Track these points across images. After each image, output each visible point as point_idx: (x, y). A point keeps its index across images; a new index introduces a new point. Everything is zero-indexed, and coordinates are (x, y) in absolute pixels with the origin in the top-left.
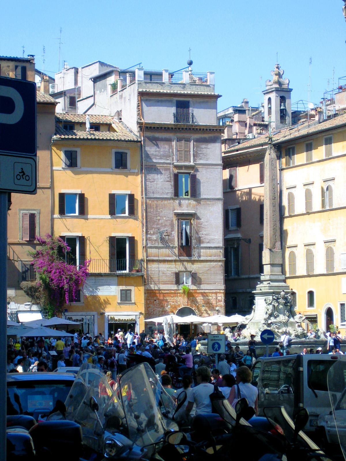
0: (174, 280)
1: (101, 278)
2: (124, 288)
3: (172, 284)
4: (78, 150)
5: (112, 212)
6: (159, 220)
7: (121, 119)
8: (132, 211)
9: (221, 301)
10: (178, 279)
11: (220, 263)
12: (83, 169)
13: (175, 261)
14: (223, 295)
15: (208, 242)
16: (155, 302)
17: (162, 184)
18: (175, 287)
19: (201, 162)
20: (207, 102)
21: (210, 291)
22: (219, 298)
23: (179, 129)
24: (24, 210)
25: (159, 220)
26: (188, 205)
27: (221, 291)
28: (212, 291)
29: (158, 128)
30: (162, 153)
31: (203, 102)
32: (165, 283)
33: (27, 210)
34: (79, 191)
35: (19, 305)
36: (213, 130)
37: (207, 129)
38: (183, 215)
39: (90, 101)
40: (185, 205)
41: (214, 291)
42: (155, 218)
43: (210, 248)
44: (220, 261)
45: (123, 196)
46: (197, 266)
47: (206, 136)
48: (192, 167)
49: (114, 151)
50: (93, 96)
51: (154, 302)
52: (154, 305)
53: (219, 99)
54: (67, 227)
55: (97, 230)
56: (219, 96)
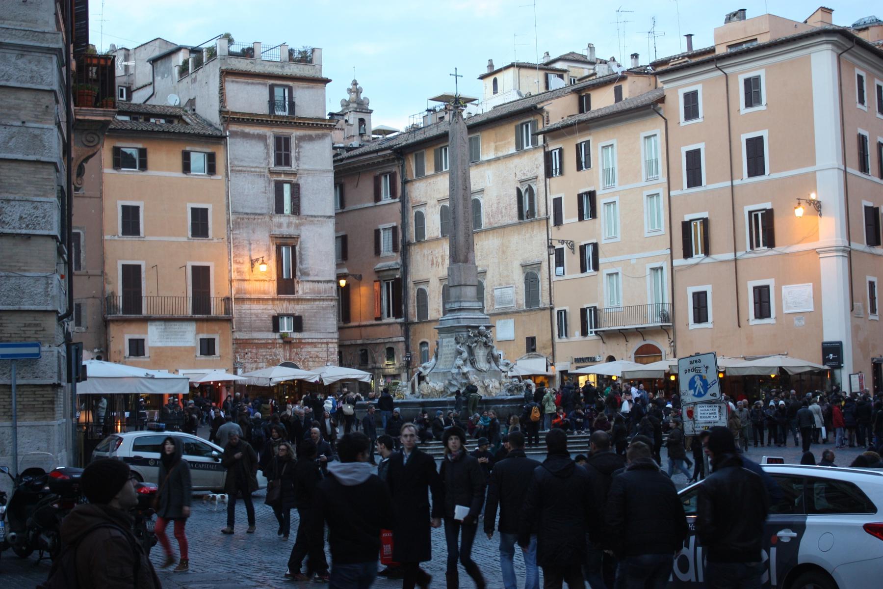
0: (271, 325)
3: (269, 331)
7: (194, 110)
13: (273, 299)
14: (336, 346)
15: (317, 275)
19: (306, 167)
20: (312, 88)
22: (331, 350)
26: (289, 225)
27: (334, 341)
31: (308, 88)
32: (260, 330)
39: (148, 91)
40: (285, 225)
41: (325, 341)
43: (318, 282)
47: (313, 133)
48: (294, 174)
50: (152, 83)
53: (328, 85)
56: (327, 81)
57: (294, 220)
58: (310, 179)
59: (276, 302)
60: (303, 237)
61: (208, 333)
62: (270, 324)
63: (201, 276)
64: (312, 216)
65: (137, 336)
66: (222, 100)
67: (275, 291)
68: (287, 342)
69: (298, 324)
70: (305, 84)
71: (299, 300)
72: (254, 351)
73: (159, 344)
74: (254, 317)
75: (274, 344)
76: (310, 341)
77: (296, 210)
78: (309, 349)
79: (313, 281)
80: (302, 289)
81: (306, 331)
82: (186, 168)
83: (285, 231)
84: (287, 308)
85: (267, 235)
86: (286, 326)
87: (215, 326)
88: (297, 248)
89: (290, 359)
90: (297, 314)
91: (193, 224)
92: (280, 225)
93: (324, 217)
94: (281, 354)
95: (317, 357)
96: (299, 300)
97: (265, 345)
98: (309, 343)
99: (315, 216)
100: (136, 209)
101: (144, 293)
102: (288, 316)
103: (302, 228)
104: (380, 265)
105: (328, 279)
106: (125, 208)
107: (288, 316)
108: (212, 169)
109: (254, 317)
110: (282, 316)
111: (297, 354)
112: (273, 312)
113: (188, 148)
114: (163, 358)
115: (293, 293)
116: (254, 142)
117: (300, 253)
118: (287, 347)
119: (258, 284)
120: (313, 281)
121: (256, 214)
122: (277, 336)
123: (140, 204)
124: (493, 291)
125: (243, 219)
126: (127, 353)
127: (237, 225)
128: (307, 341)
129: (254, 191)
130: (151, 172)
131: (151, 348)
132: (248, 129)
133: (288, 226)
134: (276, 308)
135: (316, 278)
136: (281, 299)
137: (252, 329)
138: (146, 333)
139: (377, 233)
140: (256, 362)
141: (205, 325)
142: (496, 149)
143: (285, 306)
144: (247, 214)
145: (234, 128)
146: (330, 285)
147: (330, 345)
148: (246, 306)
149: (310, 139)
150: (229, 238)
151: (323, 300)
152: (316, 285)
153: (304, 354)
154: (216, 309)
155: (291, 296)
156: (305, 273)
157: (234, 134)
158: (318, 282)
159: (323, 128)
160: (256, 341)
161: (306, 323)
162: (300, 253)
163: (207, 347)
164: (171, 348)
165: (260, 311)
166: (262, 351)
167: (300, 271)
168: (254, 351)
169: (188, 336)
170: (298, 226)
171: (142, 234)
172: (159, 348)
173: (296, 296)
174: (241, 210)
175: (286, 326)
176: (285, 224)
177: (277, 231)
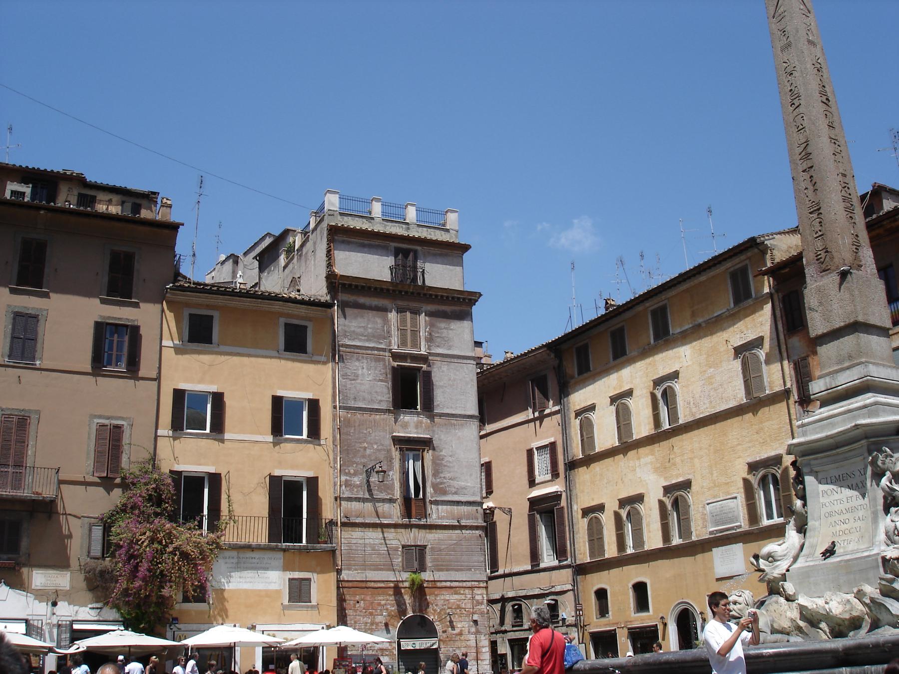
1: (250, 554)
2: (297, 575)
4: (216, 314)
5: (277, 429)
6: (365, 448)
8: (315, 432)
9: (482, 603)
11: (478, 532)
12: (222, 348)
13: (396, 526)
15: (456, 493)
16: (357, 605)
17: (372, 383)
20: (446, 255)
21: (461, 584)
22: (478, 597)
23: (400, 292)
24: (100, 417)
25: (365, 448)
26: (418, 425)
28: (464, 584)
29: (363, 287)
30: (370, 330)
31: (441, 255)
33: (108, 418)
34: (214, 388)
35: (76, 608)
36: (459, 298)
37: (447, 297)
40: (412, 425)
41: (469, 584)
42: (357, 445)
43: (458, 503)
44: (477, 528)
45: (297, 404)
46: (437, 536)
47: (447, 308)
48: (424, 359)
49: (282, 321)
51: (355, 605)
52: (355, 611)
53: (466, 256)
54: (189, 455)
55: (245, 463)
66: (330, 265)
70: (437, 251)
72: (368, 598)
76: (448, 584)
80: (437, 514)
84: (415, 538)
92: (405, 426)
95: (459, 607)
104: (536, 492)
124: (704, 507)
128: (444, 584)
134: (400, 537)
135: (456, 498)
137: (364, 567)
139: (530, 453)
140: (371, 614)
142: (694, 315)
147: (476, 591)
148: (357, 534)
153: (440, 603)
163: (299, 592)
164: (246, 591)
167: (434, 486)
173: (429, 521)
174: (352, 404)
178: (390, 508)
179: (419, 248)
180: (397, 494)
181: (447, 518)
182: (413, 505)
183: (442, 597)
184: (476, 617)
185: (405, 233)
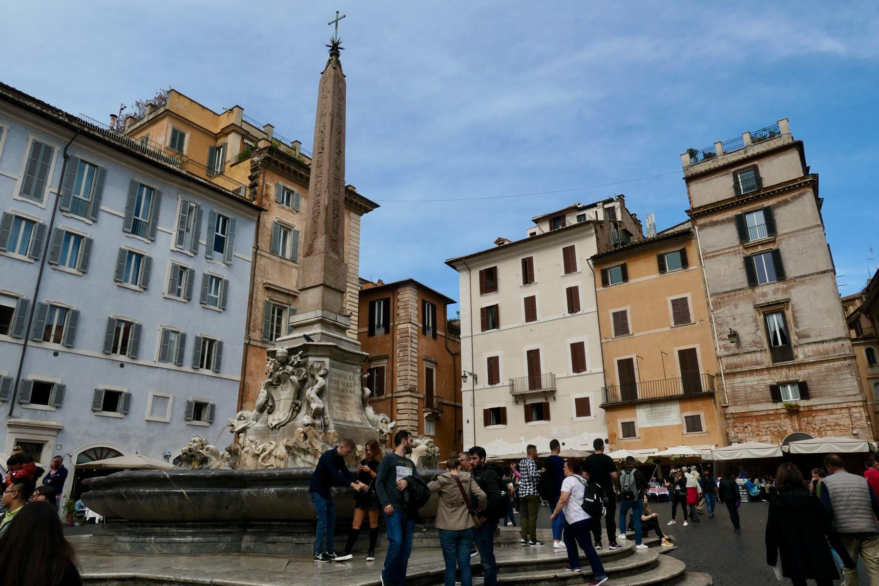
2: (689, 414)
3: (768, 402)
9: (860, 420)
10: (775, 393)
13: (768, 369)
15: (819, 335)
18: (772, 406)
21: (836, 406)
27: (858, 404)
28: (840, 406)
32: (758, 402)
38: (769, 305)
40: (771, 293)
41: (845, 405)
43: (822, 342)
47: (787, 197)
57: (781, 285)
58: (793, 241)
59: (772, 371)
60: (793, 301)
61: (692, 410)
62: (768, 394)
63: (688, 358)
64: (801, 277)
65: (628, 420)
67: (770, 360)
68: (793, 411)
69: (804, 390)
71: (800, 365)
73: (648, 425)
74: (748, 389)
75: (777, 414)
76: (824, 407)
77: (780, 274)
78: (823, 416)
79: (815, 343)
80: (800, 354)
81: (813, 397)
82: (662, 269)
83: (771, 298)
84: (787, 376)
85: (752, 306)
86: (791, 395)
87: (699, 404)
88: (789, 313)
89: (801, 429)
90: (801, 380)
91: (674, 314)
92: (764, 295)
93: (818, 273)
94: (789, 426)
95: (837, 424)
96: (800, 365)
97: (767, 417)
98: (822, 410)
99: (805, 276)
100: (624, 313)
101: (637, 381)
102: (792, 383)
103: (792, 290)
105: (836, 336)
106: (615, 315)
107: (792, 383)
108: (685, 264)
109: (748, 389)
110: (784, 384)
111: (808, 423)
112: (770, 382)
113: (662, 252)
114: (652, 436)
115: (792, 358)
116: (723, 227)
117: (794, 317)
118: (795, 417)
119: (748, 356)
120: (815, 343)
121: (736, 290)
122: (779, 406)
123: (627, 308)
125: (723, 298)
126: (621, 435)
127: (717, 305)
128: (819, 408)
129: (730, 271)
130: (632, 281)
131: (641, 429)
132: (715, 218)
133: (774, 293)
134: (773, 377)
136: (777, 368)
137: (748, 402)
138: (636, 416)
140: (758, 435)
141: (688, 405)
143: (784, 373)
144: (726, 292)
145: (702, 221)
146: (840, 343)
147: (853, 410)
148: (738, 380)
149: (786, 202)
150: (711, 319)
151: (833, 360)
152: (821, 346)
153: (817, 422)
154: (705, 387)
155: (790, 363)
156: (801, 336)
157: (702, 227)
158: (822, 342)
159: (798, 189)
160: (756, 414)
161: (813, 388)
162: (794, 317)
163: (693, 424)
164: (659, 428)
165: (755, 383)
166: (765, 424)
167: (797, 334)
168: (754, 424)
169: (673, 416)
170: (785, 291)
171: (631, 333)
172: (648, 428)
173: (796, 361)
174: (720, 291)
175: (791, 395)
176: (769, 291)
177: (762, 301)
178: (761, 357)
179: (756, 163)
180: (766, 346)
181: (814, 356)
182: (782, 350)
183: (820, 418)
184: (855, 432)
185: (745, 156)
